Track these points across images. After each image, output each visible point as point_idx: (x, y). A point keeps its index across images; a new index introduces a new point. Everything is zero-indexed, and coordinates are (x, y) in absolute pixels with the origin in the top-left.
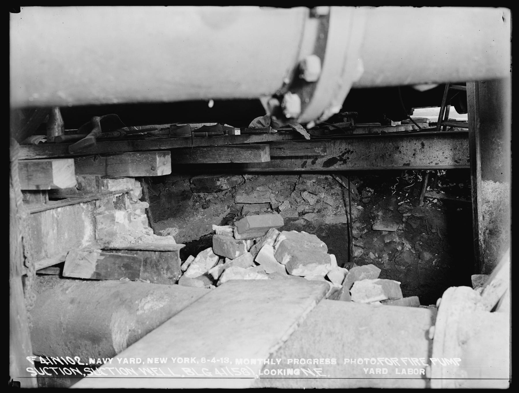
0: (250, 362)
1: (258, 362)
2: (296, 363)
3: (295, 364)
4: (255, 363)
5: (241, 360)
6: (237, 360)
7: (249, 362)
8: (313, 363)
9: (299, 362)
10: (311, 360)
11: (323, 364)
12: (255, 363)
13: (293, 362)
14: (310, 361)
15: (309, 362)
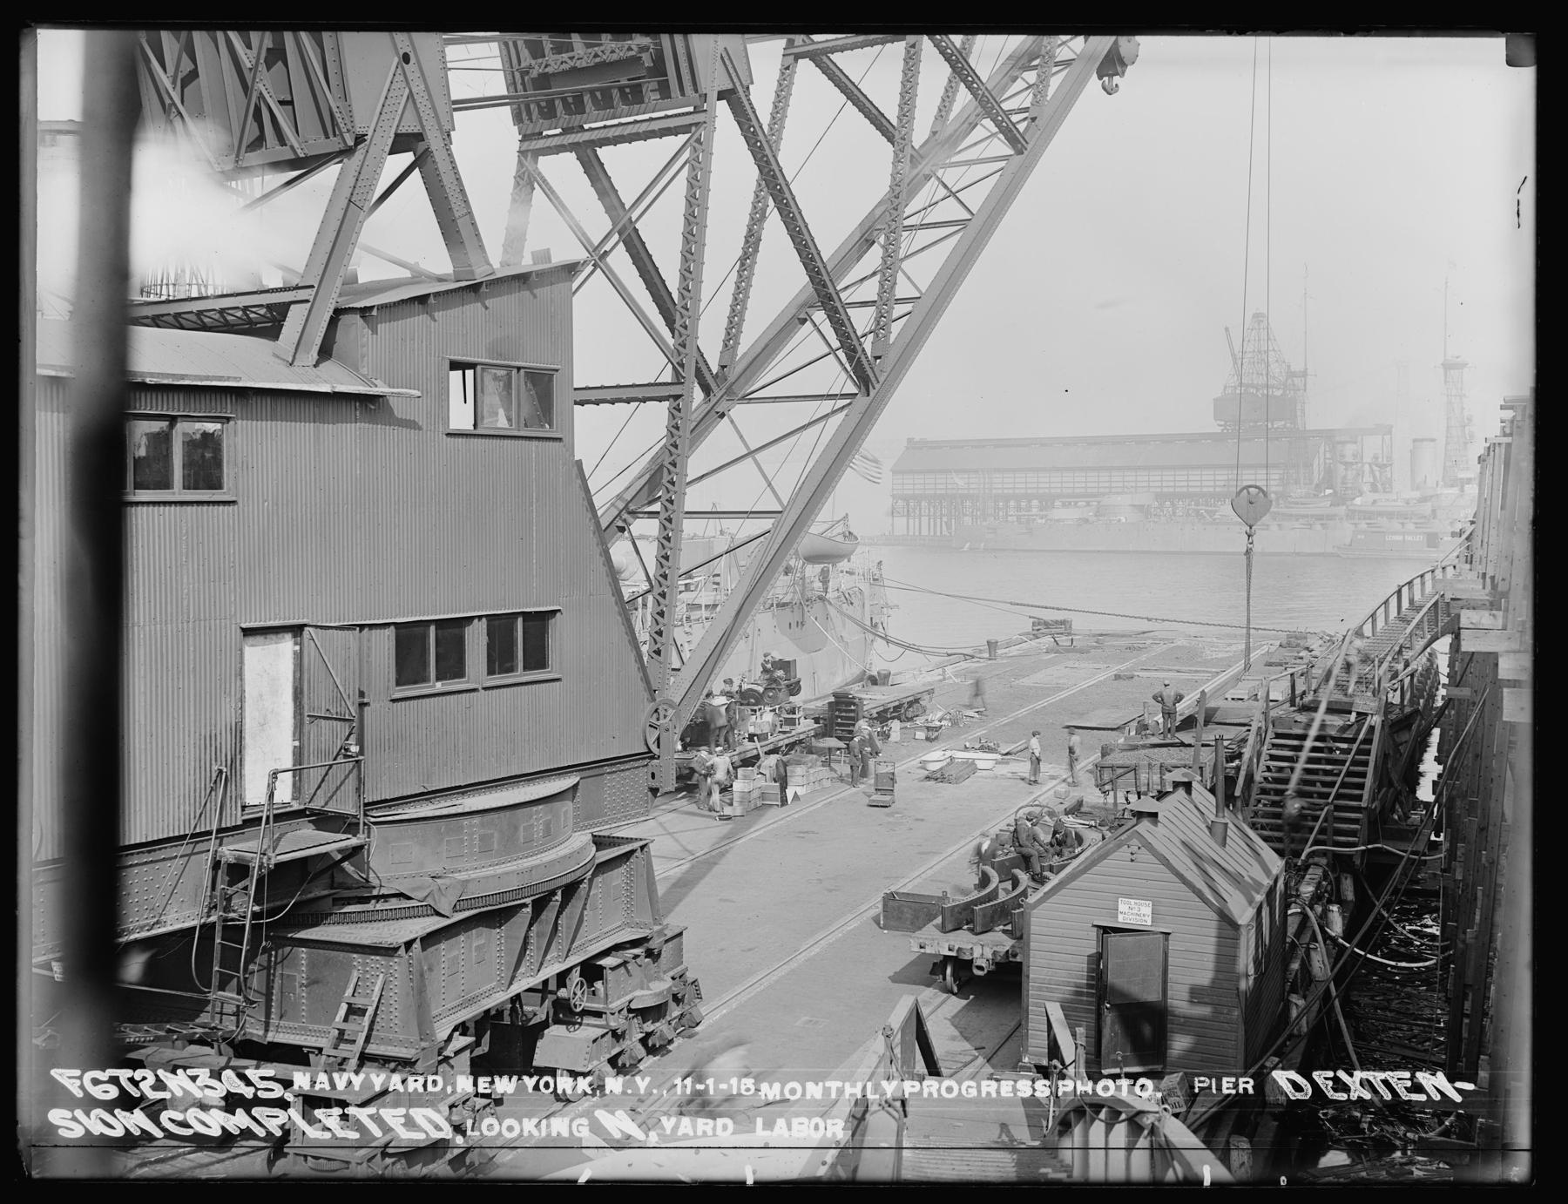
0: (804, 1094)
1: (827, 1091)
2: (930, 1094)
3: (925, 1095)
4: (818, 1096)
5: (777, 1086)
6: (764, 1087)
7: (798, 1095)
8: (979, 1091)
9: (939, 1090)
10: (972, 1083)
11: (1012, 1095)
12: (818, 1096)
13: (922, 1089)
14: (969, 1087)
15: (970, 1090)
